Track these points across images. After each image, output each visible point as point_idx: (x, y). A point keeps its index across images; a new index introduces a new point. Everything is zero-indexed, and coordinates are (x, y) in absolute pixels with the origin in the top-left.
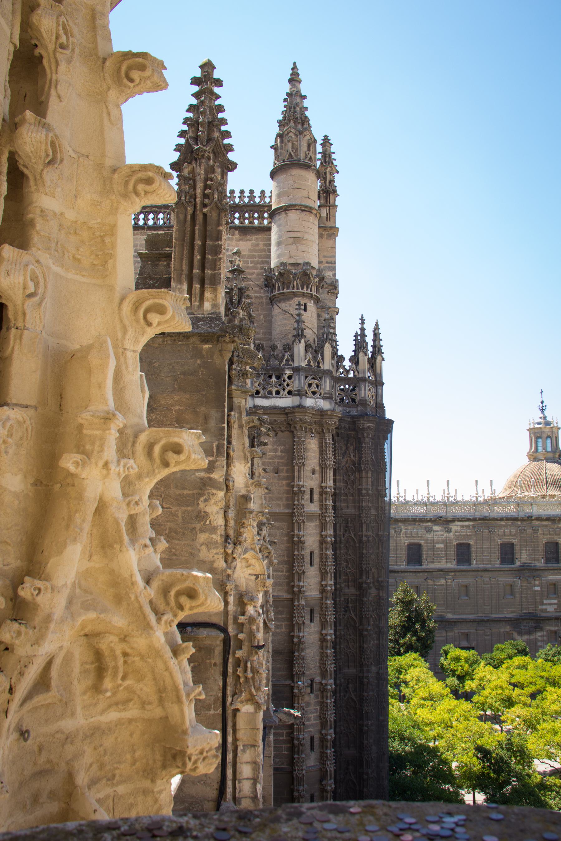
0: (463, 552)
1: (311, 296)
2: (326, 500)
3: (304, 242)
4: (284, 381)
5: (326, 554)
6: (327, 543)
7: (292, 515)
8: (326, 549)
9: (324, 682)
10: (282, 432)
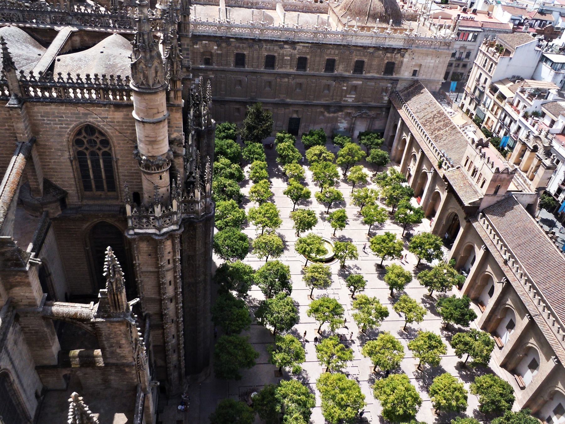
0: (302, 63)
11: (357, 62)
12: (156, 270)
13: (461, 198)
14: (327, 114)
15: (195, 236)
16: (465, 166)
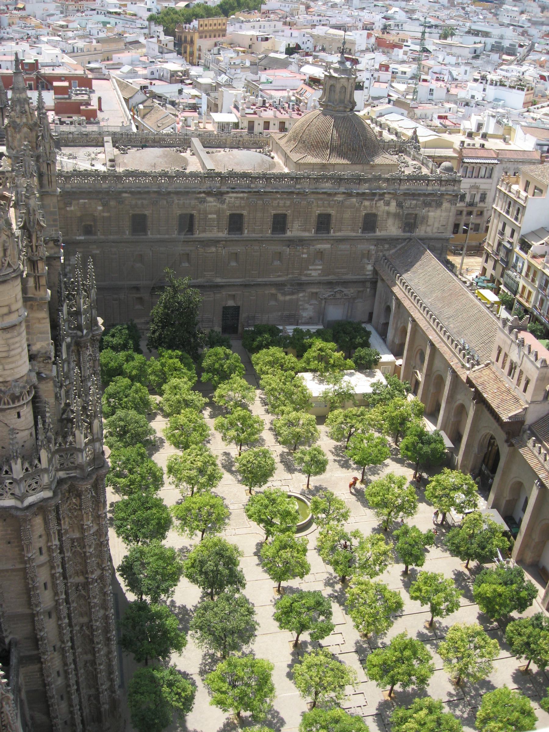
0: (236, 223)
3: (10, 360)
11: (320, 215)
12: (21, 566)
13: (496, 410)
14: (280, 297)
15: (81, 506)
16: (497, 361)
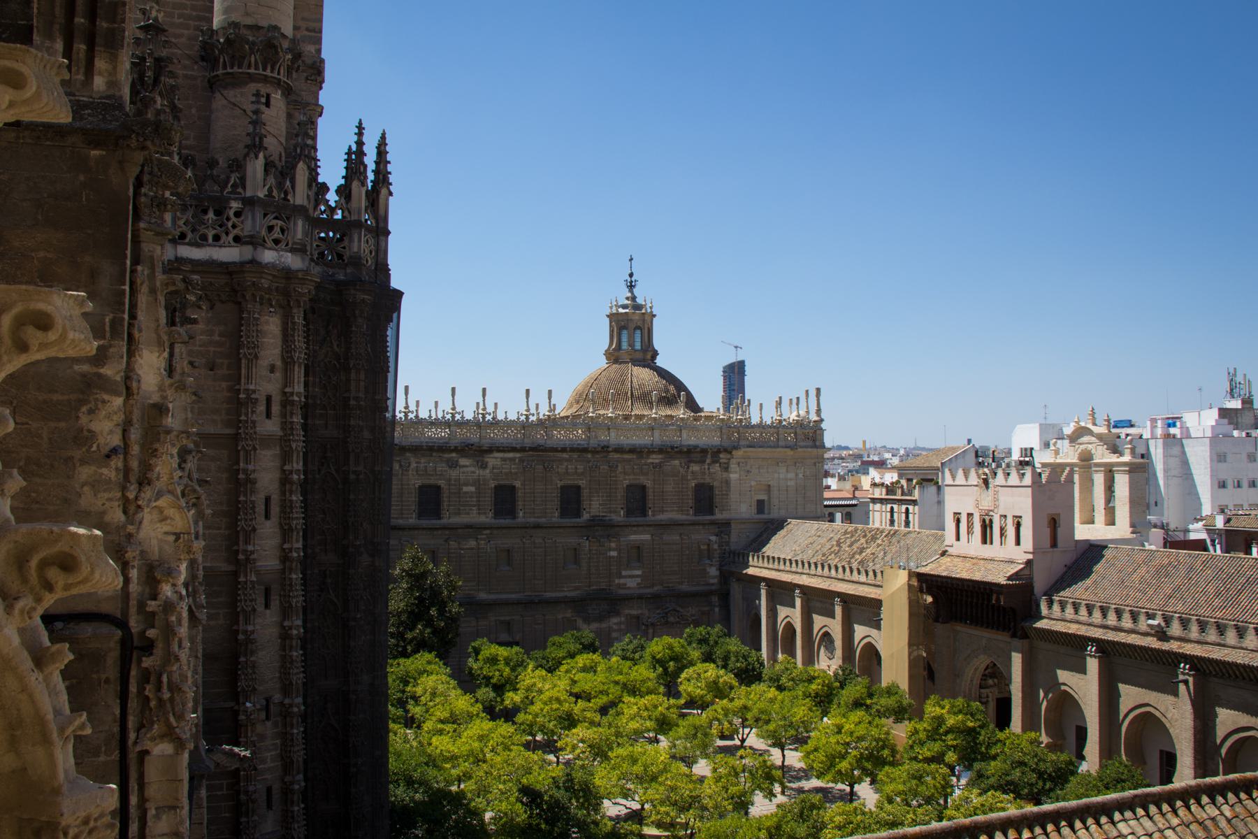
0: (505, 500)
1: (278, 83)
2: (292, 414)
4: (228, 219)
5: (291, 501)
6: (292, 483)
7: (236, 438)
8: (291, 492)
9: (287, 701)
10: (222, 302)
